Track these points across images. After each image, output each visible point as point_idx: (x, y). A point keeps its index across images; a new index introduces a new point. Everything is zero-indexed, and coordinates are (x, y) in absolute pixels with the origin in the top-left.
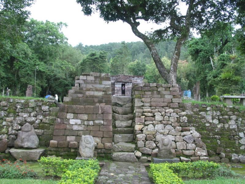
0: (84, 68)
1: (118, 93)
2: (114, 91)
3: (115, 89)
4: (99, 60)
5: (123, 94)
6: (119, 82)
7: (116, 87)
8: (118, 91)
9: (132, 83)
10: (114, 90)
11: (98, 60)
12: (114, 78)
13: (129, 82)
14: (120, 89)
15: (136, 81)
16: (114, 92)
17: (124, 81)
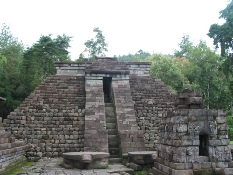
0: (29, 62)
1: (95, 101)
2: (85, 96)
3: (87, 90)
4: (56, 48)
5: (108, 104)
6: (96, 73)
7: (89, 85)
8: (95, 94)
9: (128, 76)
10: (84, 93)
11: (54, 49)
12: (84, 68)
13: (120, 74)
14: (98, 91)
16: (85, 99)
17: (109, 70)
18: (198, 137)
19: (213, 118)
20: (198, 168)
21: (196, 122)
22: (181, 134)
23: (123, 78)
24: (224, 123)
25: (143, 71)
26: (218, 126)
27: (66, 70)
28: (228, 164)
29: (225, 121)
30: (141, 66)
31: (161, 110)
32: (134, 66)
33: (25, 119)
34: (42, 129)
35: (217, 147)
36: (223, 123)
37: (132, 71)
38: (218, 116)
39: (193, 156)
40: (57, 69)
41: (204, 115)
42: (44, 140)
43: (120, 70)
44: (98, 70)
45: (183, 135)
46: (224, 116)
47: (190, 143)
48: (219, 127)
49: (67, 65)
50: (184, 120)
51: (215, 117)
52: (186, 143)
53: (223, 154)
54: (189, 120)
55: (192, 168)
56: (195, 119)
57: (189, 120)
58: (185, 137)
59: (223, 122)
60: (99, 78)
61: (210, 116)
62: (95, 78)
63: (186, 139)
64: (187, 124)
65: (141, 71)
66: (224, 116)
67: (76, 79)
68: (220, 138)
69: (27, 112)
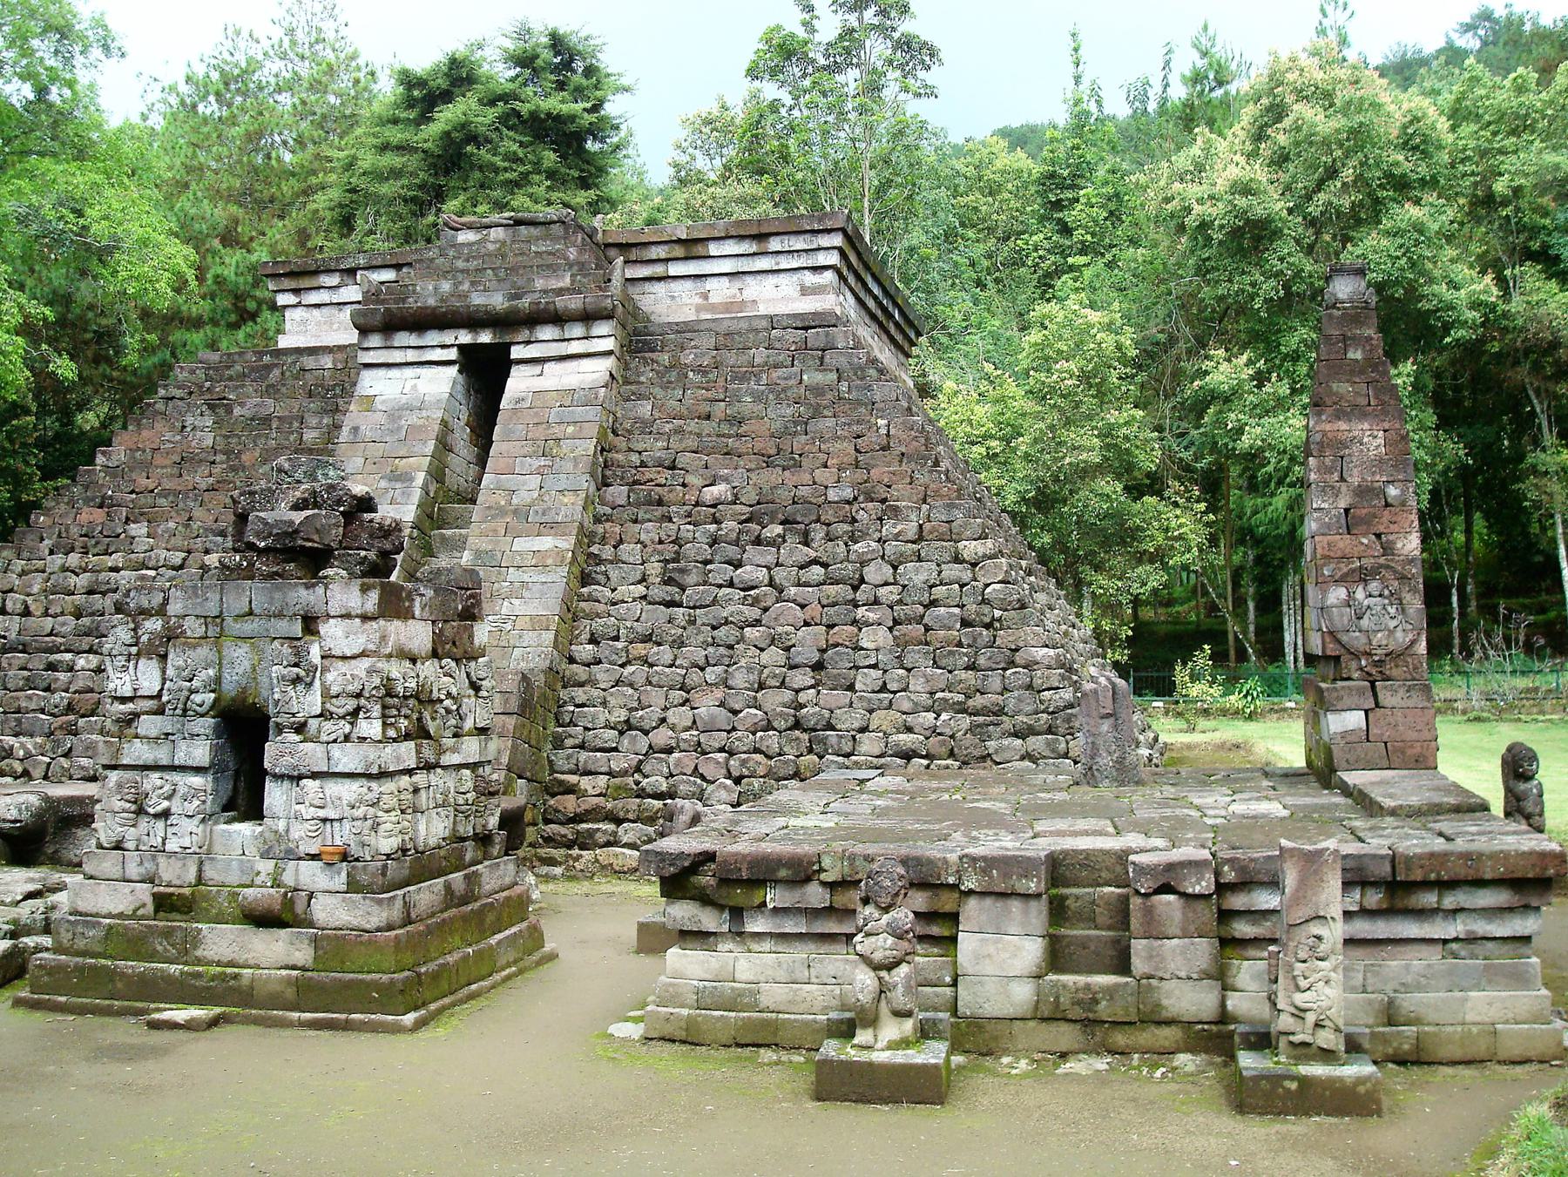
6: (423, 322)
13: (558, 319)
15: (728, 306)
17: (497, 301)
18: (206, 725)
19: (297, 628)
20: (178, 883)
21: (204, 652)
22: (122, 707)
23: (575, 347)
24: (363, 654)
25: (796, 277)
26: (325, 670)
27: (334, 310)
28: (344, 874)
29: (372, 647)
30: (775, 244)
31: (772, 543)
32: (731, 247)
33: (19, 608)
34: (81, 662)
35: (304, 781)
36: (353, 657)
37: (725, 279)
38: (329, 616)
39: (173, 820)
40: (285, 307)
41: (257, 611)
42: (72, 717)
43: (560, 292)
44: (431, 302)
45: (137, 715)
46: (365, 618)
47: (162, 755)
48: (330, 677)
49: (334, 280)
50: (145, 638)
51: (310, 623)
52: (137, 752)
53: (341, 820)
54: (171, 636)
55: (150, 880)
56: (201, 631)
57: (171, 636)
58: (149, 725)
59: (356, 651)
60: (438, 355)
61: (280, 615)
62: (411, 356)
63: (154, 733)
64: (164, 657)
65: (782, 279)
66: (365, 618)
67: (330, 365)
68: (324, 738)
69: (37, 571)
